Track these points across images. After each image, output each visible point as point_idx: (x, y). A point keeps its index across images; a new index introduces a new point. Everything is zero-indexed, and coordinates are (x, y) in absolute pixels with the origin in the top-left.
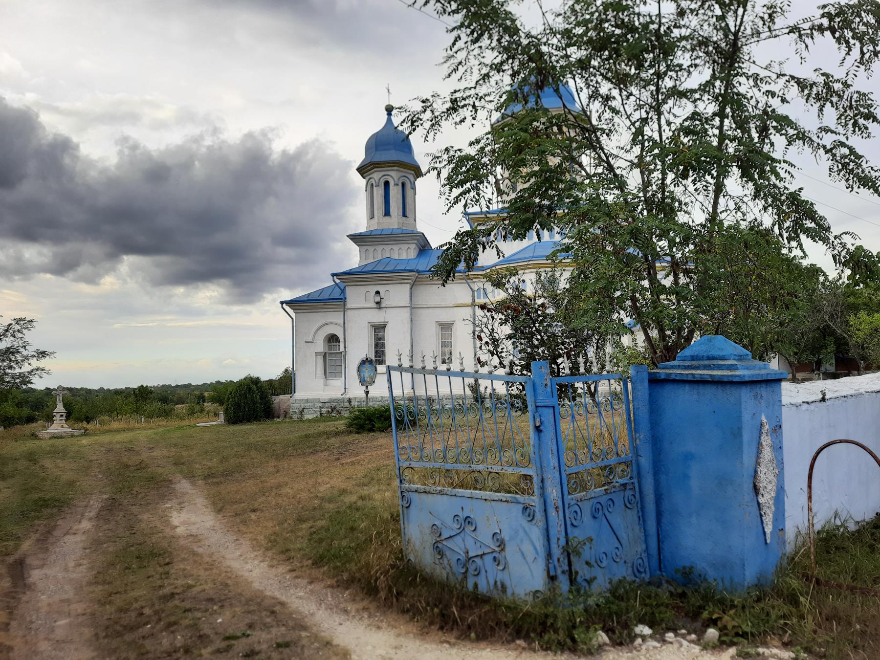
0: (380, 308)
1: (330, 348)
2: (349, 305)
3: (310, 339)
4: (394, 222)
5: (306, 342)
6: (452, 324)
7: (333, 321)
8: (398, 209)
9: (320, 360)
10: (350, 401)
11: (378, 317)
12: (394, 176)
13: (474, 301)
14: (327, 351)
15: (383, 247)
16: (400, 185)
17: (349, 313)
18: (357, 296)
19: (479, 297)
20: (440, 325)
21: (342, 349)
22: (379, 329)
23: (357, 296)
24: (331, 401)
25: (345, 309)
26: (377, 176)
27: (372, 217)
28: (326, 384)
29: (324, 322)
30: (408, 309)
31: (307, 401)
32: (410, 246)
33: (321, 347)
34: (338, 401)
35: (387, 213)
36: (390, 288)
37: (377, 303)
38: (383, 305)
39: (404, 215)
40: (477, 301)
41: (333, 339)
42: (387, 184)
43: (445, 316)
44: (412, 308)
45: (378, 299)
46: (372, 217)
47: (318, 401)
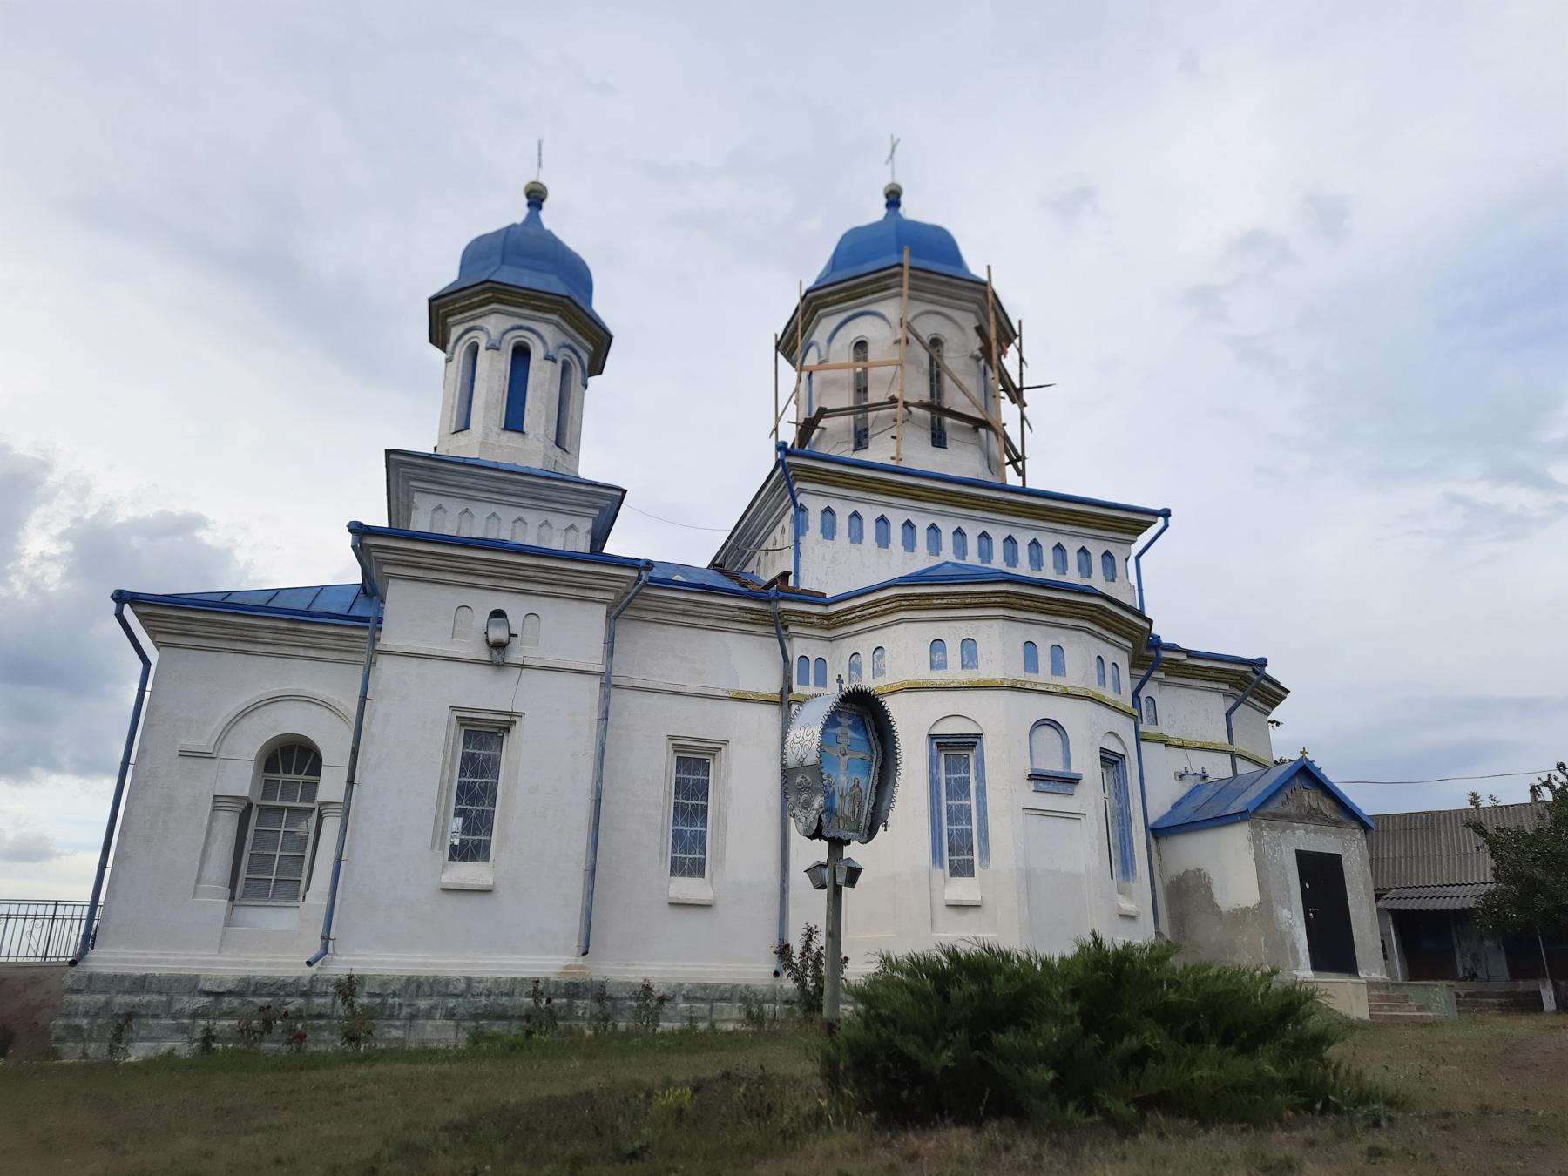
0: (500, 666)
1: (269, 788)
2: (388, 640)
3: (204, 742)
5: (186, 754)
6: (714, 752)
7: (309, 690)
8: (548, 421)
9: (227, 825)
10: (348, 987)
11: (488, 693)
12: (546, 337)
13: (787, 688)
14: (257, 800)
15: (495, 508)
16: (559, 364)
17: (385, 665)
18: (418, 614)
19: (804, 681)
20: (676, 748)
22: (482, 738)
23: (418, 614)
24: (248, 988)
25: (373, 654)
26: (494, 324)
28: (229, 922)
29: (274, 689)
30: (597, 681)
31: (141, 984)
32: (577, 521)
33: (240, 779)
34: (278, 988)
35: (514, 422)
37: (499, 646)
38: (514, 656)
39: (559, 442)
40: (796, 688)
41: (292, 758)
42: (521, 354)
43: (697, 722)
44: (608, 683)
45: (498, 634)
47: (191, 985)
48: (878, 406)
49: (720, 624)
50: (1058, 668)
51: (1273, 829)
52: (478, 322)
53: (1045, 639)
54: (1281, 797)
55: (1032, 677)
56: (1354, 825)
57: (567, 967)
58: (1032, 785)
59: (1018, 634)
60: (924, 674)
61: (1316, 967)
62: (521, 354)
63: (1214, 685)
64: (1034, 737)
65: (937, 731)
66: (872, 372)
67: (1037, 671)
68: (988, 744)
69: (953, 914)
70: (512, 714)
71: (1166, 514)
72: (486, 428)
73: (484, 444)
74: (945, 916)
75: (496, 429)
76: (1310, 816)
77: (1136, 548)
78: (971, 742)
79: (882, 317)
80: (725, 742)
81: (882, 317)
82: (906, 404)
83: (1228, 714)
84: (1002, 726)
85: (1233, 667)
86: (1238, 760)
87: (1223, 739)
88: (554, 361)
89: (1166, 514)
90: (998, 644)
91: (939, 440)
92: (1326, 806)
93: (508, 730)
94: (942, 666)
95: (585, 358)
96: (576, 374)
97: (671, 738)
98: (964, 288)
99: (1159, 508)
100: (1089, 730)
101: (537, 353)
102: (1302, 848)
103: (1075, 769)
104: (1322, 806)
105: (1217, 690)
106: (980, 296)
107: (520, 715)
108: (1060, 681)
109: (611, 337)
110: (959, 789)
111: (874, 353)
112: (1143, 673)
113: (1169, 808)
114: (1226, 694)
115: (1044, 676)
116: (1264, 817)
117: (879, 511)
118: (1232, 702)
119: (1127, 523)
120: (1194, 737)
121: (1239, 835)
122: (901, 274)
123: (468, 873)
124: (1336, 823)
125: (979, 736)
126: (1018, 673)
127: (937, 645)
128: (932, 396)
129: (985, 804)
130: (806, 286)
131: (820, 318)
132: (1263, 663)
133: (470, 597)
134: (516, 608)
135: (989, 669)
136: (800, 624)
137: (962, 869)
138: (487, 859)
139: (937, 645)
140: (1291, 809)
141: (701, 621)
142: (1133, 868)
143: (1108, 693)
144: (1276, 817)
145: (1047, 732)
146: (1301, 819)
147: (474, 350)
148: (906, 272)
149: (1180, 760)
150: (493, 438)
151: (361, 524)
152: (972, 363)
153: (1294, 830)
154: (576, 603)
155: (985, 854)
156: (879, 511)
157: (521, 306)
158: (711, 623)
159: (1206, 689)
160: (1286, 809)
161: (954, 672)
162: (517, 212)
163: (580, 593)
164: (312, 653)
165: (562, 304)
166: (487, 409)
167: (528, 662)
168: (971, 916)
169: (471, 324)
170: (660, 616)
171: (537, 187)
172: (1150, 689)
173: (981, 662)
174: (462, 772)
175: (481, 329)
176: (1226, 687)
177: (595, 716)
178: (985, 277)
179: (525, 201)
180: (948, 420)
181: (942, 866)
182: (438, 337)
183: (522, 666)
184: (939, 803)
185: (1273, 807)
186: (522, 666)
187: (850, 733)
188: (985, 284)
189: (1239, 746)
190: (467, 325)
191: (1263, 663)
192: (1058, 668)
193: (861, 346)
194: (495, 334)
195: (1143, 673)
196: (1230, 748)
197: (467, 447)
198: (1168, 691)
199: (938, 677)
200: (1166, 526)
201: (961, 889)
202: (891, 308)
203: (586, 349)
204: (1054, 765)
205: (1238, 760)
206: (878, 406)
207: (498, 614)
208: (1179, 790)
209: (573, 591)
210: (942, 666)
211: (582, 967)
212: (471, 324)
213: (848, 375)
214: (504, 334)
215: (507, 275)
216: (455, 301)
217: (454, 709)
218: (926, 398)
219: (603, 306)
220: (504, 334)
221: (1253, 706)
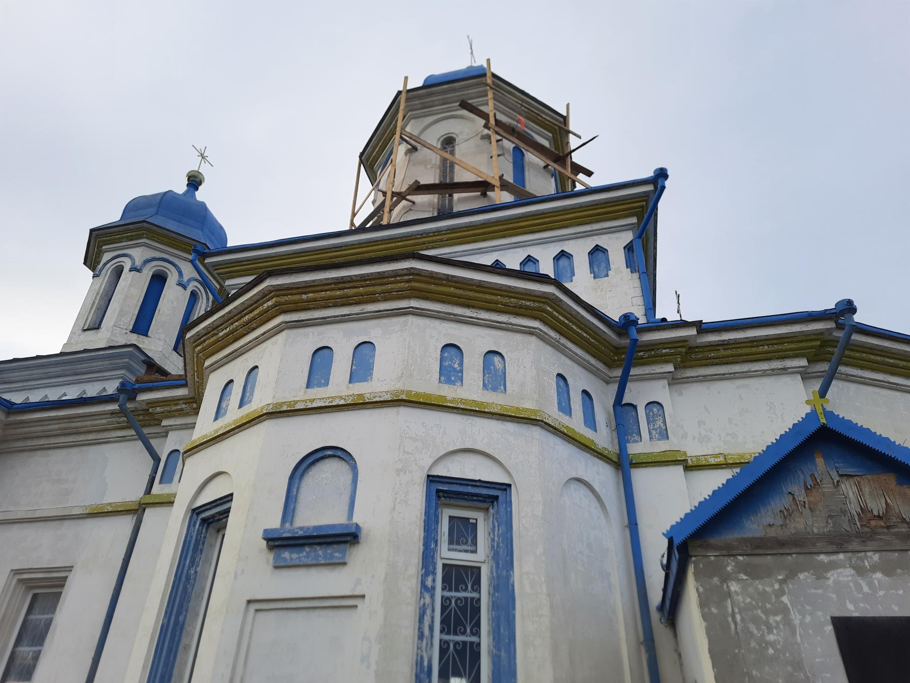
43: (40, 549)
49: (100, 436)
51: (755, 573)
59: (306, 341)
65: (200, 502)
80: (70, 569)
85: (796, 328)
97: (16, 572)
102: (852, 610)
105: (784, 371)
112: (618, 373)
114: (806, 376)
116: (729, 551)
118: (817, 386)
132: (848, 307)
136: (170, 415)
141: (82, 438)
146: (838, 542)
153: (820, 572)
158: (91, 437)
159: (764, 374)
160: (799, 524)
165: (143, 229)
170: (42, 442)
172: (640, 394)
176: (803, 362)
185: (760, 523)
191: (848, 307)
195: (618, 373)
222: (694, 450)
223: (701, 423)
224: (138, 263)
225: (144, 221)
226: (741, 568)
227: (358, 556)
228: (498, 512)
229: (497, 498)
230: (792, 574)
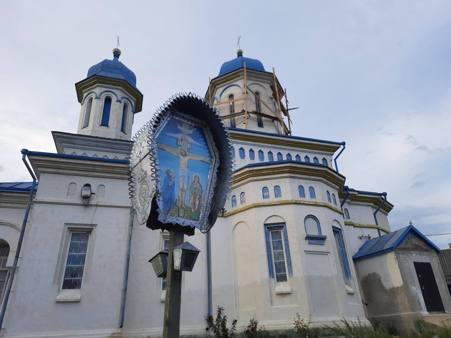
0: (87, 206)
2: (39, 197)
4: (112, 132)
8: (118, 122)
11: (81, 217)
12: (117, 94)
17: (37, 208)
21: (10, 262)
22: (80, 234)
23: (54, 188)
27: (86, 125)
30: (128, 211)
35: (105, 122)
36: (107, 183)
37: (86, 198)
38: (93, 201)
45: (86, 193)
46: (86, 125)
48: (239, 114)
50: (313, 195)
51: (403, 254)
52: (93, 90)
53: (307, 185)
54: (405, 241)
55: (303, 199)
56: (433, 251)
57: (113, 334)
58: (307, 241)
59: (297, 183)
60: (261, 200)
61: (429, 310)
62: (108, 101)
63: (368, 204)
64: (306, 222)
65: (268, 222)
66: (236, 103)
67: (305, 197)
68: (288, 225)
69: (279, 297)
70: (92, 225)
71: (344, 144)
72: (94, 125)
73: (93, 131)
74: (276, 299)
75: (98, 125)
76: (416, 248)
77: (334, 157)
78: (282, 226)
79: (238, 86)
81: (238, 86)
82: (248, 113)
83: (375, 214)
84: (292, 217)
85: (374, 196)
86: (380, 231)
87: (373, 223)
88: (120, 102)
89: (344, 144)
90: (288, 187)
91: (260, 125)
92: (421, 244)
93: (90, 232)
94: (268, 197)
95: (133, 103)
96: (130, 109)
98: (265, 75)
99: (341, 142)
100: (327, 220)
101: (114, 99)
102: (416, 261)
103: (323, 234)
104: (420, 244)
105: (369, 206)
106: (271, 79)
107: (95, 225)
108: (314, 200)
109: (143, 96)
110: (278, 245)
111: (235, 98)
112: (343, 200)
113: (358, 250)
114: (373, 207)
115: (307, 198)
117: (240, 146)
118: (375, 210)
119: (331, 147)
120: (363, 223)
121: (391, 257)
122: (243, 71)
123: (71, 294)
124: (426, 250)
125: (284, 223)
126: (297, 198)
127: (265, 189)
128: (257, 109)
129: (289, 250)
130: (211, 79)
131: (217, 89)
132: (385, 194)
133: (75, 179)
134: (94, 183)
135: (287, 196)
137: (282, 278)
138: (79, 287)
139: (265, 189)
140: (409, 246)
142: (350, 274)
143: (332, 205)
144: (404, 249)
145: (311, 220)
147: (91, 100)
148: (245, 70)
149: (359, 232)
150: (97, 128)
151: (27, 150)
152: (270, 100)
153: (412, 254)
154: (120, 180)
155: (291, 271)
156: (240, 146)
157: (108, 84)
160: (407, 246)
161: (272, 199)
162: (111, 57)
163: (122, 176)
164: (8, 205)
165: (124, 84)
166: (95, 118)
167: (99, 204)
168: (287, 298)
169: (91, 91)
171: (117, 50)
172: (346, 206)
173: (283, 194)
174: (70, 251)
175: (93, 92)
177: (128, 224)
178: (272, 72)
179: (113, 55)
180: (263, 118)
181: (273, 278)
182: (80, 99)
183: (97, 206)
184: (270, 251)
185: (402, 245)
186: (97, 206)
187: (190, 140)
188: (272, 74)
189: (380, 226)
190: (89, 92)
191: (385, 194)
192: (313, 195)
193: (231, 96)
194: (98, 94)
195: (343, 200)
196: (377, 226)
197: (87, 132)
198: (352, 207)
199: (266, 201)
200: (344, 148)
201: (282, 287)
202: (241, 83)
203: (133, 100)
204: (314, 232)
205: (380, 231)
206: (239, 114)
207: (88, 185)
208: (360, 243)
209: (118, 176)
210: (268, 197)
211: (120, 333)
212: (91, 91)
213: (227, 105)
214: (102, 93)
215: (103, 74)
216: (84, 84)
217: (66, 224)
218: (255, 110)
219: (139, 86)
220: (102, 93)
221: (382, 212)
222: (356, 222)
223: (354, 215)
224: (119, 99)
225: (125, 80)
226: (401, 253)
227: (326, 242)
228: (339, 235)
229: (338, 232)
230: (408, 254)
